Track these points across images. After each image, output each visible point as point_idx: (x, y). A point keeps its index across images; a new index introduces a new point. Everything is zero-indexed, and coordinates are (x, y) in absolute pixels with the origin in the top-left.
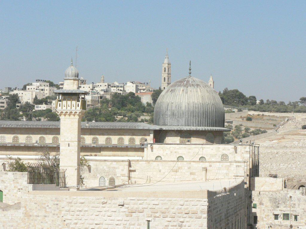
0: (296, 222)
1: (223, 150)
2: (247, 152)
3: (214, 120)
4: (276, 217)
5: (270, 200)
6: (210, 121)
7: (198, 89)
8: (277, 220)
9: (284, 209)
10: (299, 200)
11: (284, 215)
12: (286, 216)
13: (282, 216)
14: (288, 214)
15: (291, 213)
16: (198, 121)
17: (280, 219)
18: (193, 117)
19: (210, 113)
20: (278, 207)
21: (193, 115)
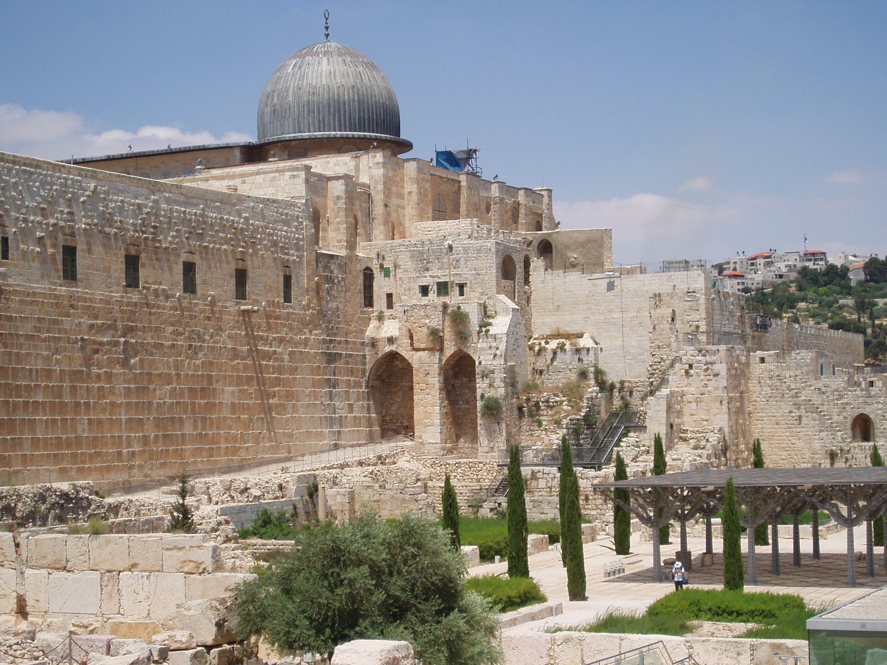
0: (461, 298)
1: (336, 165)
2: (378, 163)
3: (355, 119)
4: (425, 290)
5: (412, 256)
6: (345, 118)
7: (325, 59)
8: (426, 298)
9: (439, 273)
10: (466, 250)
11: (439, 284)
12: (443, 288)
13: (435, 287)
14: (446, 283)
15: (452, 279)
16: (319, 121)
17: (432, 296)
18: (309, 113)
19: (345, 105)
20: (427, 270)
21: (309, 110)
